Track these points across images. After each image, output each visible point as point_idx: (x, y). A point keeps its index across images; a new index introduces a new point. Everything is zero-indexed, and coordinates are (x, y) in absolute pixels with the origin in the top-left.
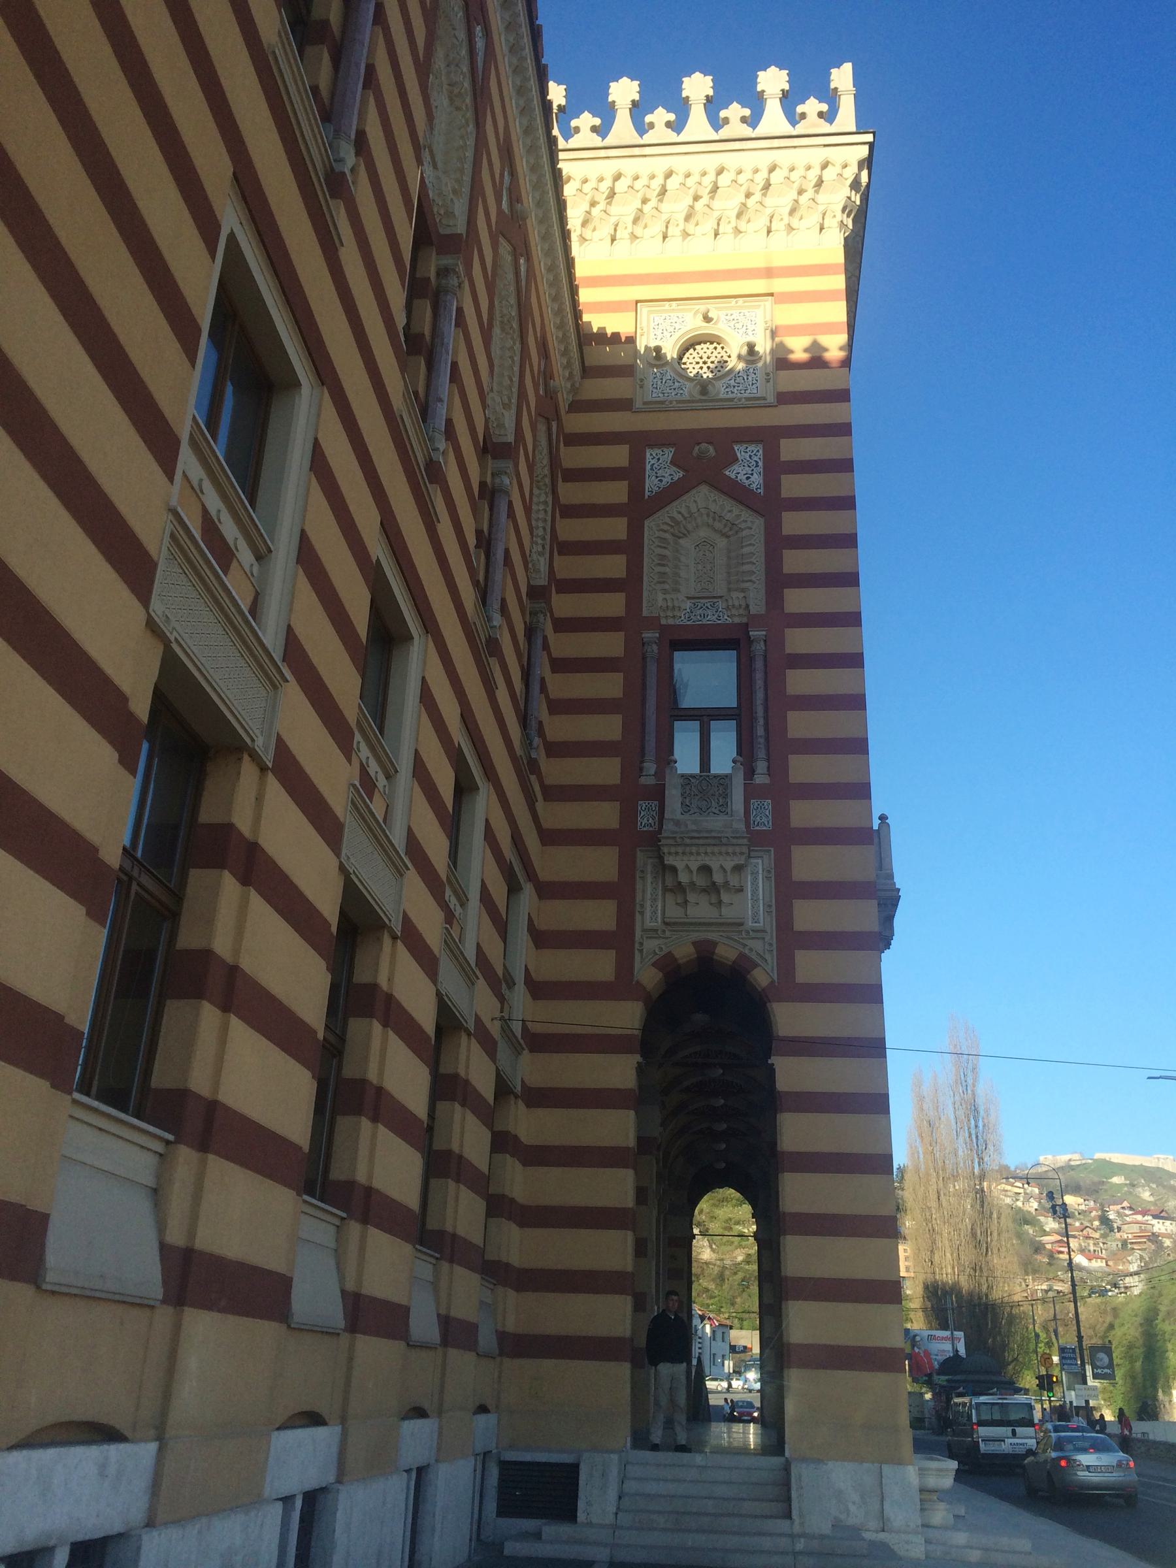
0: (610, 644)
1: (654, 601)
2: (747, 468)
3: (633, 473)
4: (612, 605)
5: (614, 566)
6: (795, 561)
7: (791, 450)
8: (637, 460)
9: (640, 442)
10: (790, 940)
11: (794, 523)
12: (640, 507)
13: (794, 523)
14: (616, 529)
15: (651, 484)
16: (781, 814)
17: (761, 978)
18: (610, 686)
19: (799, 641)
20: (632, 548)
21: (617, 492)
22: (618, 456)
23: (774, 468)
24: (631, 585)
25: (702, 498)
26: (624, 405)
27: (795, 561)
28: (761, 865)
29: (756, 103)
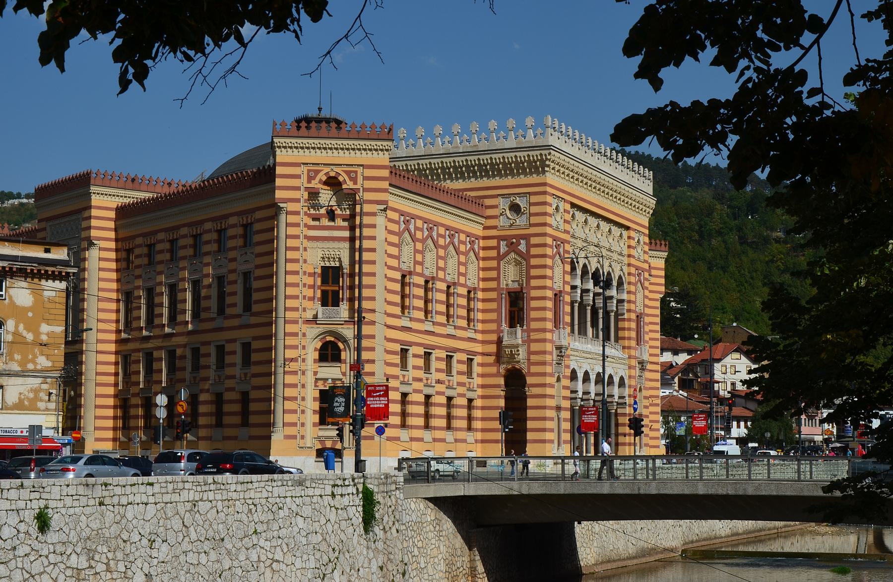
0: (493, 295)
1: (503, 285)
2: (522, 247)
3: (497, 248)
4: (493, 284)
5: (494, 274)
6: (534, 272)
7: (534, 241)
8: (499, 244)
9: (500, 238)
10: (530, 363)
11: (533, 262)
12: (500, 258)
13: (533, 262)
14: (494, 264)
15: (502, 251)
16: (529, 336)
17: (525, 371)
18: (494, 305)
19: (534, 293)
20: (498, 269)
21: (493, 253)
22: (493, 243)
23: (529, 246)
24: (497, 279)
25: (513, 255)
26: (495, 227)
27: (534, 272)
28: (525, 347)
29: (525, 129)
